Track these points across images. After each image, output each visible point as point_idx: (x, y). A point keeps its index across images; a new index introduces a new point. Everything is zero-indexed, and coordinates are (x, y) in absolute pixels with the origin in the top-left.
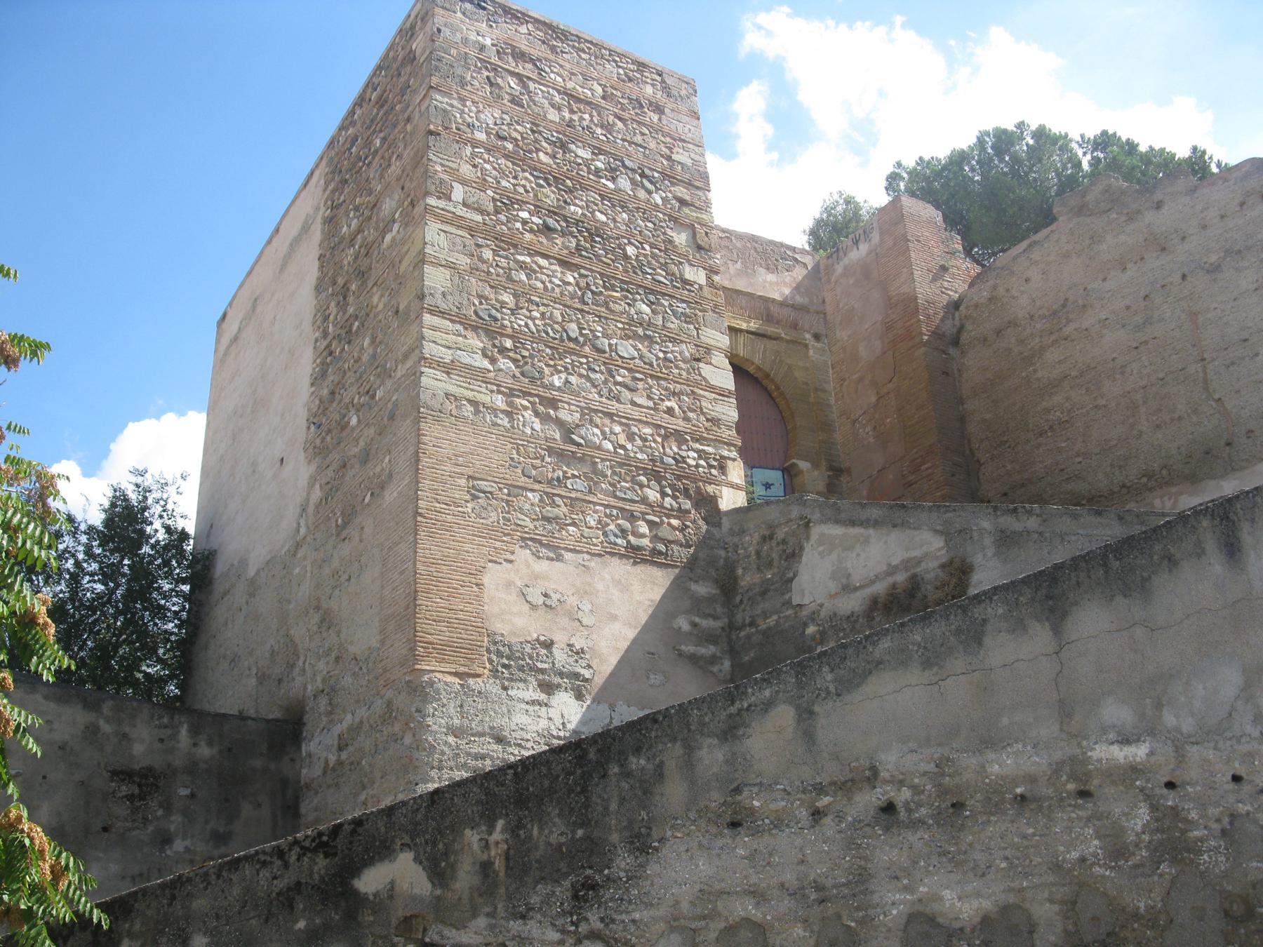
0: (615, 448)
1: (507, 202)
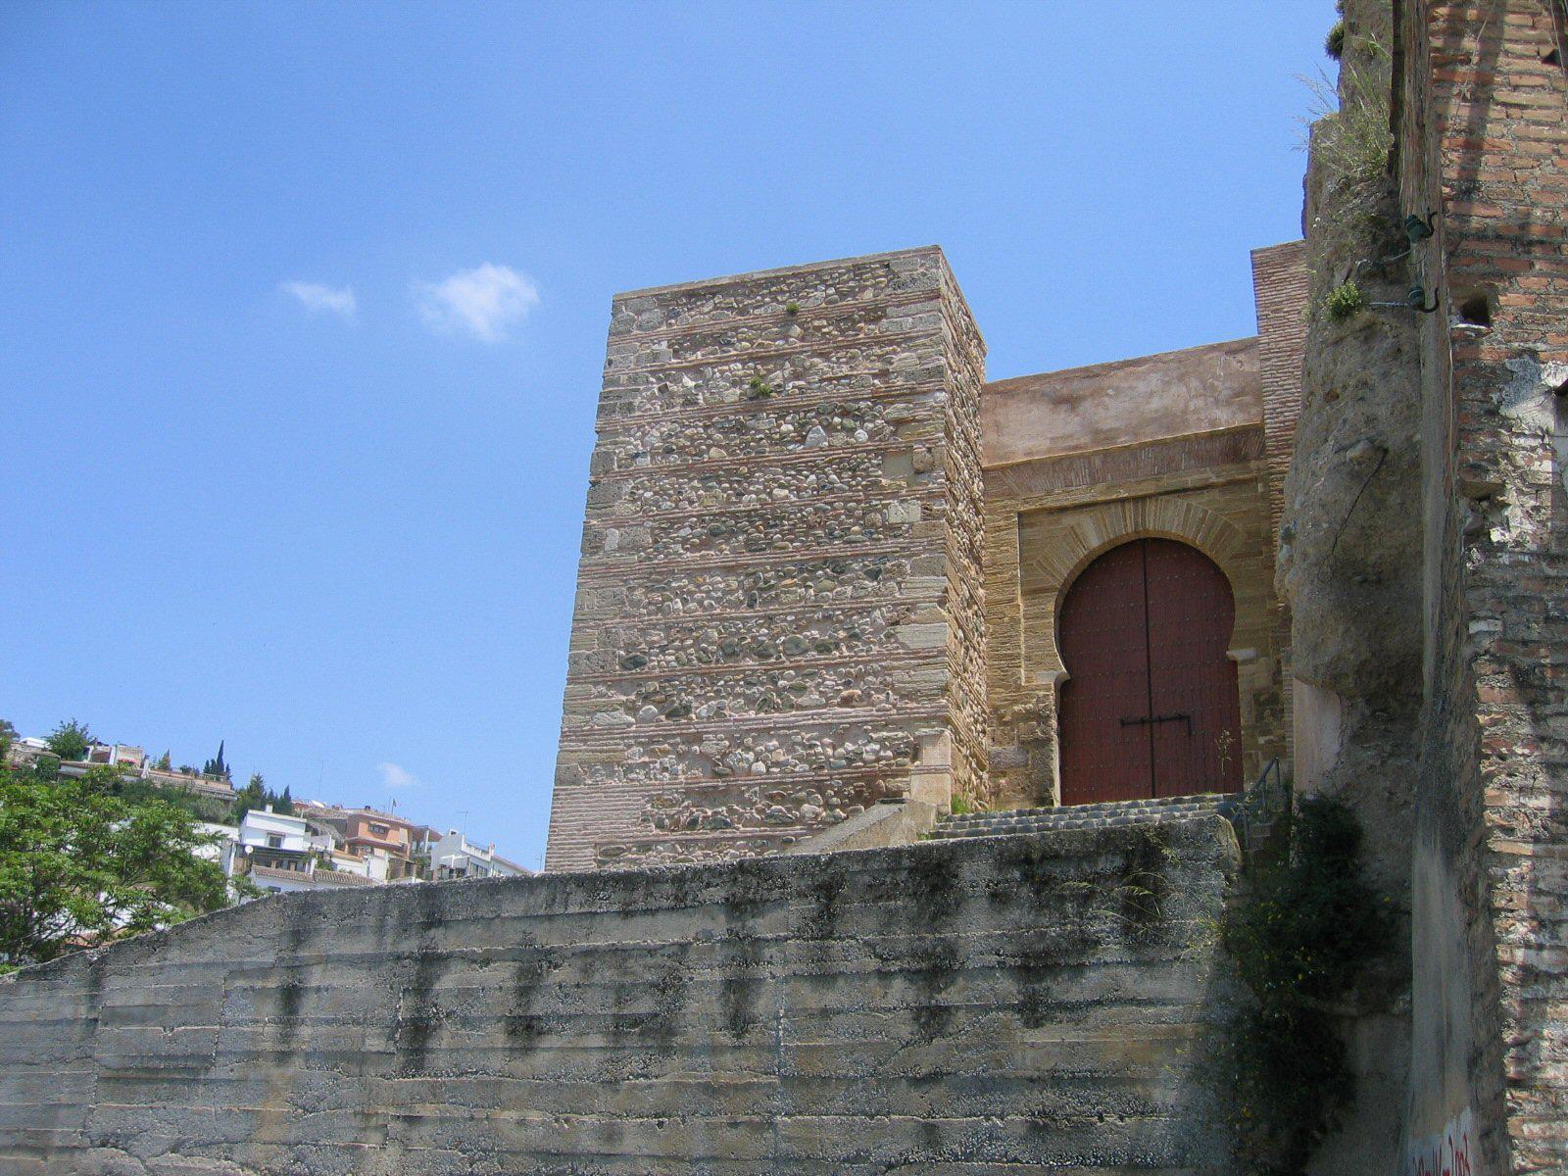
0: (768, 768)
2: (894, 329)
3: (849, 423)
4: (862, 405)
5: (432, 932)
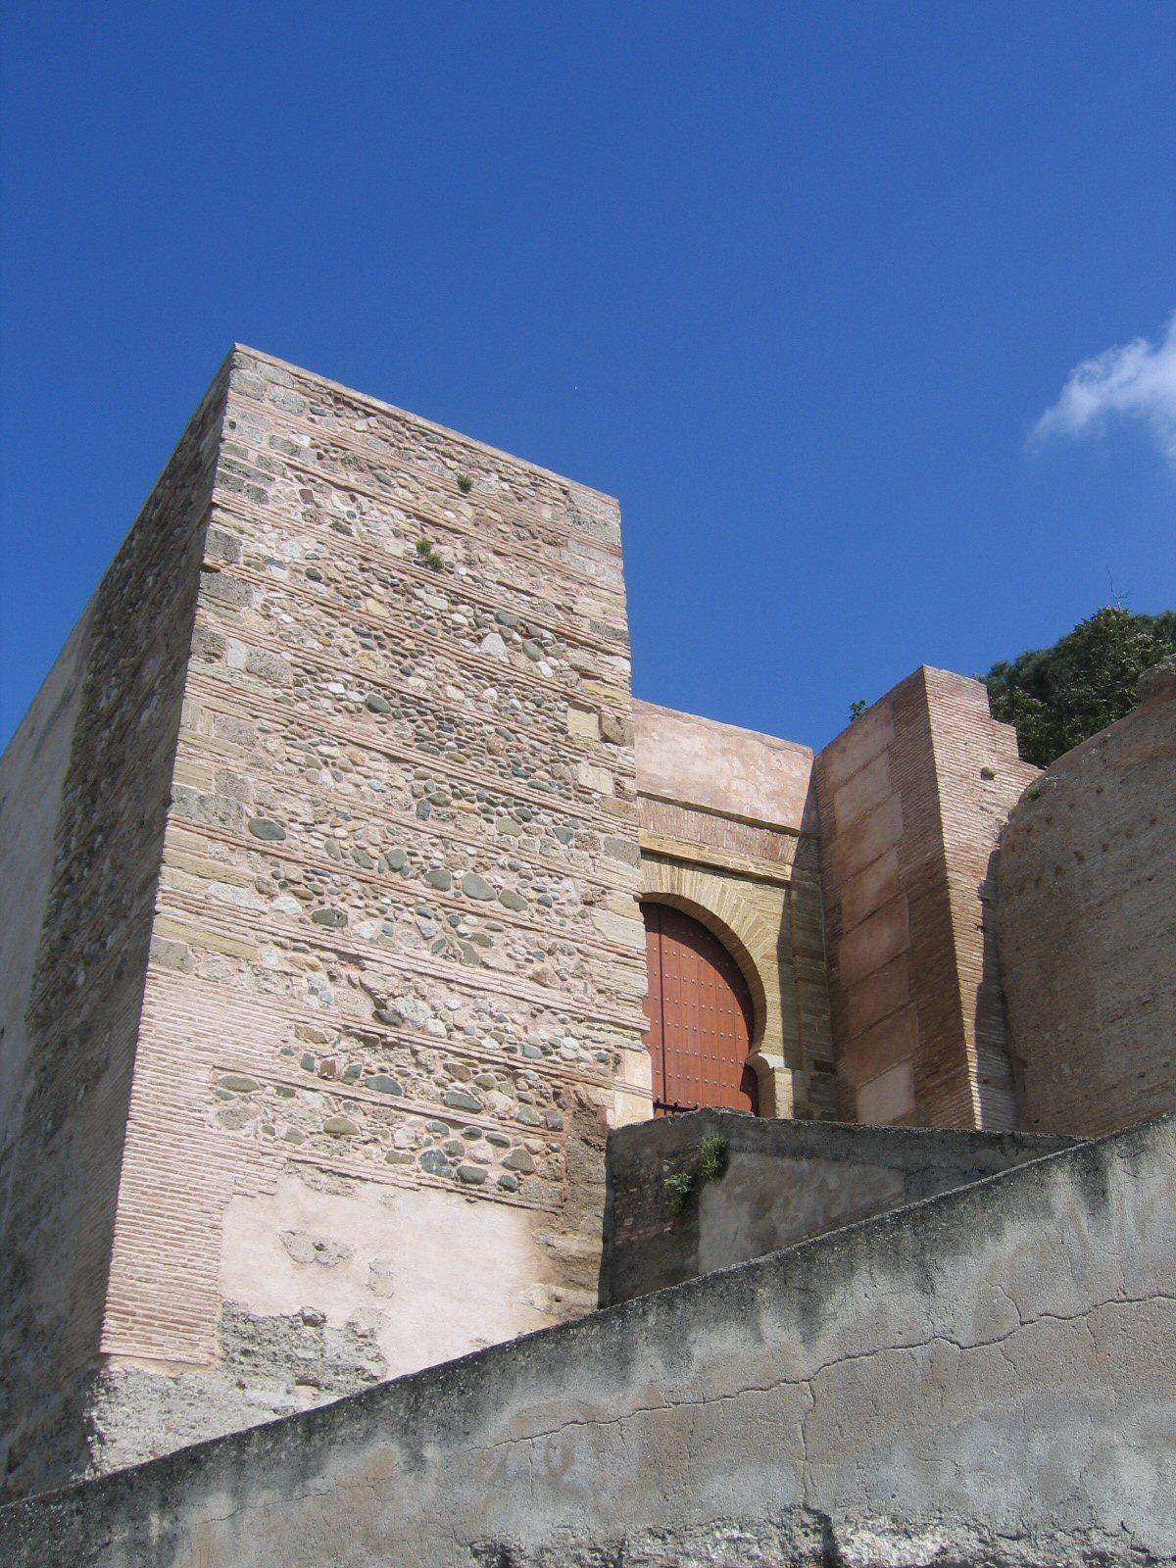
1: (313, 672)
2: (573, 566)
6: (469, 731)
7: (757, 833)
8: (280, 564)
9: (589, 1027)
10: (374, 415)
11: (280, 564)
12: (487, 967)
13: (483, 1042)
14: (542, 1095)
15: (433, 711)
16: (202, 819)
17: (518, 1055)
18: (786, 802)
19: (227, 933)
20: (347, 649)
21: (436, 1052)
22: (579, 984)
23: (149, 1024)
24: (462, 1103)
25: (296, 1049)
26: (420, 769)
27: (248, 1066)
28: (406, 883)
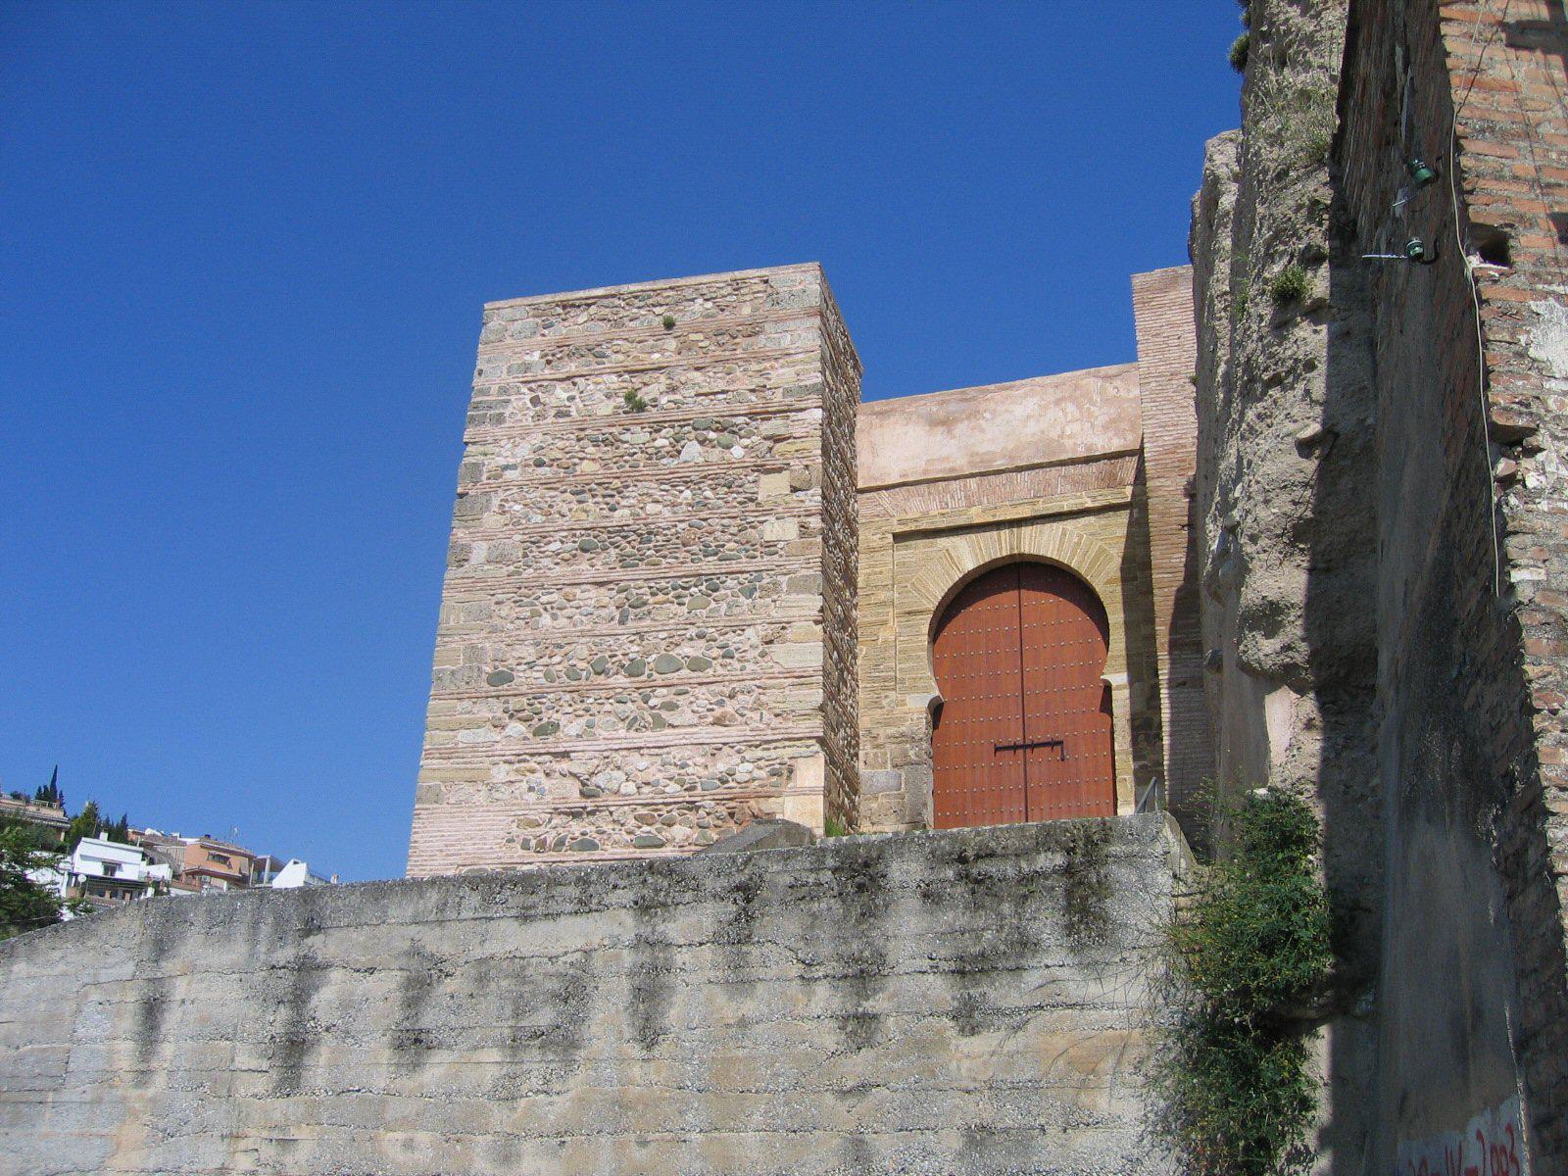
2: (770, 345)
3: (726, 437)
4: (740, 420)
5: (310, 940)
6: (665, 535)
7: (1094, 467)
8: (514, 467)
9: (764, 749)
10: (594, 304)
11: (514, 467)
12: (674, 727)
13: (667, 790)
14: (718, 818)
15: (634, 532)
16: (453, 687)
17: (699, 791)
18: (1124, 425)
19: (469, 766)
20: (565, 510)
21: (626, 808)
22: (756, 716)
23: (415, 847)
24: (647, 843)
25: (518, 836)
26: (622, 584)
27: (482, 858)
28: (611, 680)
